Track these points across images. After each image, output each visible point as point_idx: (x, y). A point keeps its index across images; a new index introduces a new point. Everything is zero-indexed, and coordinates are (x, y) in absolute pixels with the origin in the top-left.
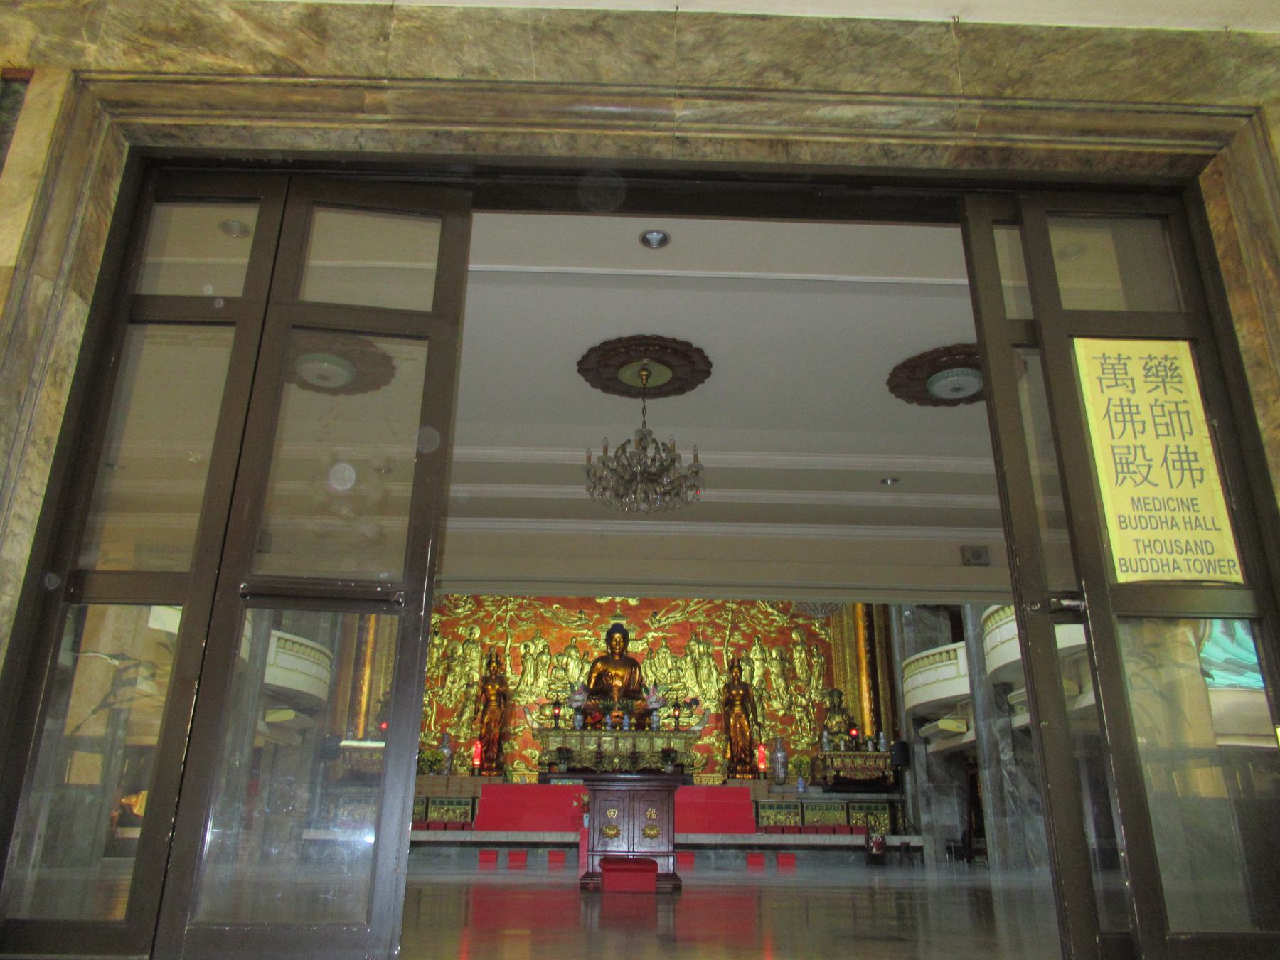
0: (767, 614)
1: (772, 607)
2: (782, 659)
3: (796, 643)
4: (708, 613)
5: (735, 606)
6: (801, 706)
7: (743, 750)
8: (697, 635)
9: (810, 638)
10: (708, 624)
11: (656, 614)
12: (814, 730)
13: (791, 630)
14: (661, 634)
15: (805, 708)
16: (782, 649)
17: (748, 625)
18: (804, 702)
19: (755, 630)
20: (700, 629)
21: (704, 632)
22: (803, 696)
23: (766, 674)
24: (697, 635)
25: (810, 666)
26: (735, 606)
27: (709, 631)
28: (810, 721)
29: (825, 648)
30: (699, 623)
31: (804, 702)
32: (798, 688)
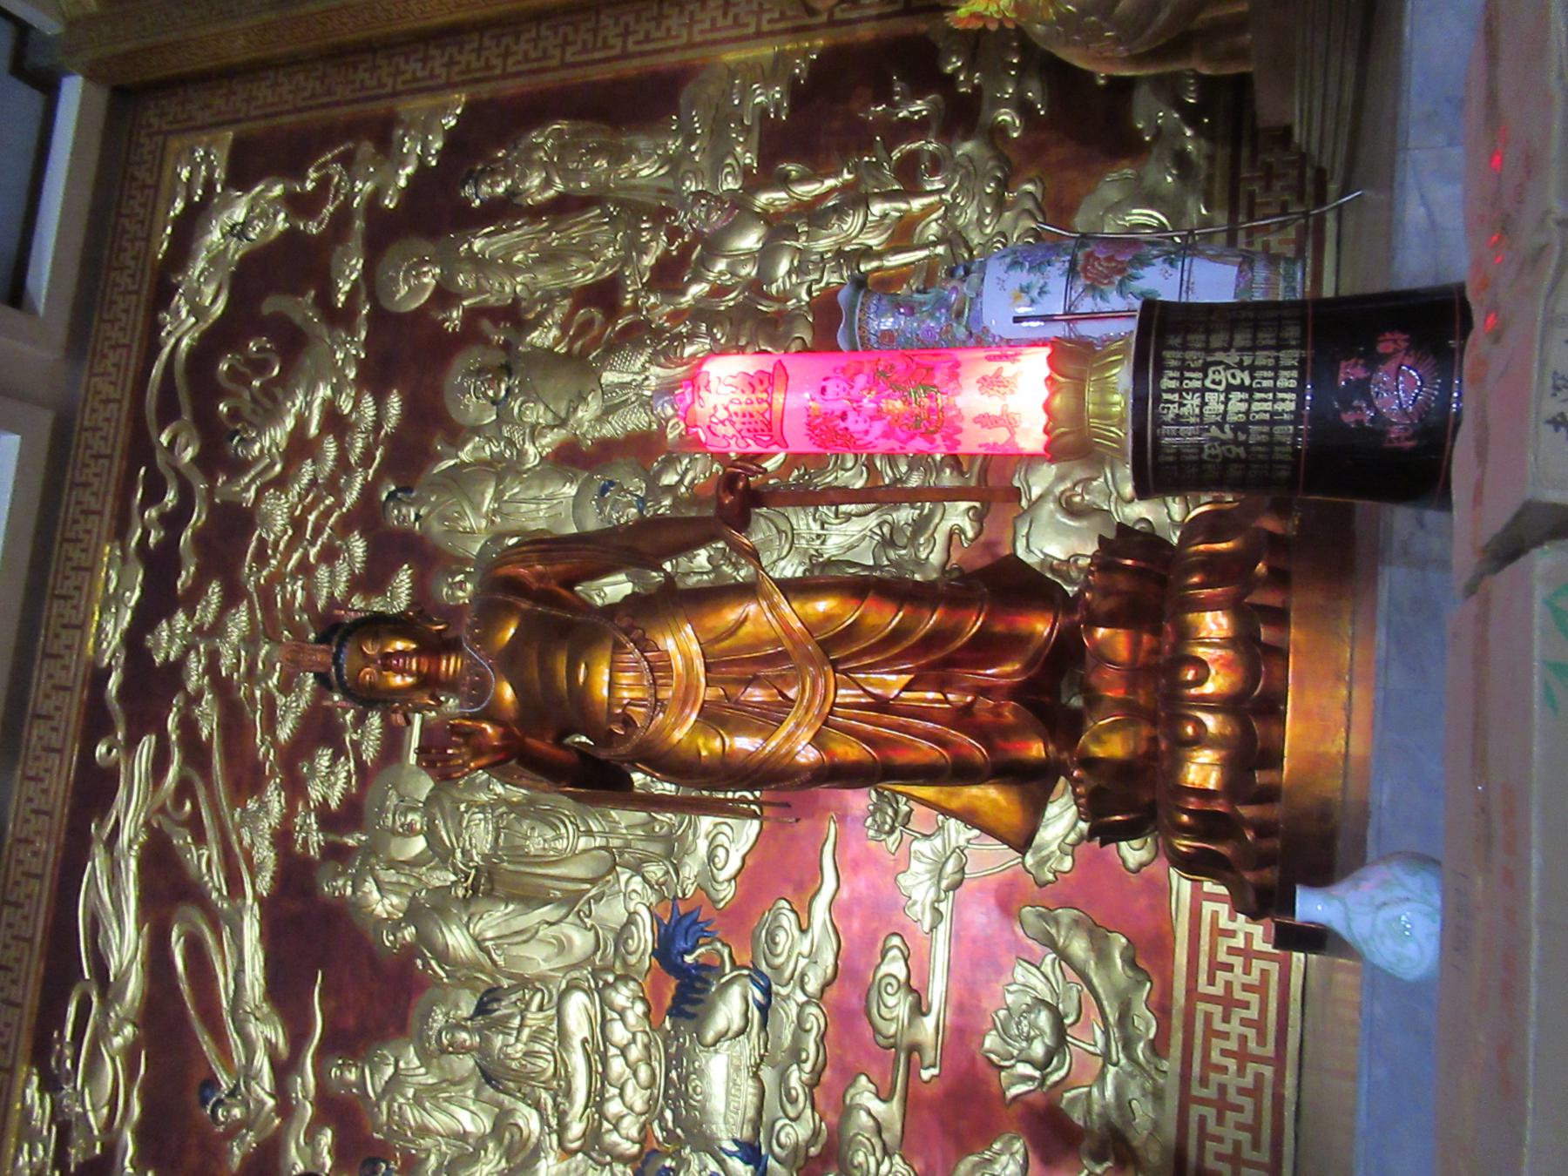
0: (300, 447)
1: (273, 415)
2: (507, 370)
3: (445, 295)
4: (247, 781)
5: (239, 624)
6: (765, 257)
7: (936, 661)
8: (336, 853)
9: (435, 212)
10: (295, 788)
11: (212, 1083)
12: (910, 178)
13: (382, 319)
14: (306, 1081)
15: (779, 227)
16: (457, 376)
17: (329, 555)
18: (750, 240)
19: (346, 526)
20: (313, 839)
21: (328, 820)
22: (713, 246)
23: (569, 459)
24: (336, 853)
25: (563, 207)
26: (239, 624)
27: (330, 781)
28: (855, 199)
29: (487, 133)
30: (283, 838)
31: (750, 240)
32: (668, 276)
